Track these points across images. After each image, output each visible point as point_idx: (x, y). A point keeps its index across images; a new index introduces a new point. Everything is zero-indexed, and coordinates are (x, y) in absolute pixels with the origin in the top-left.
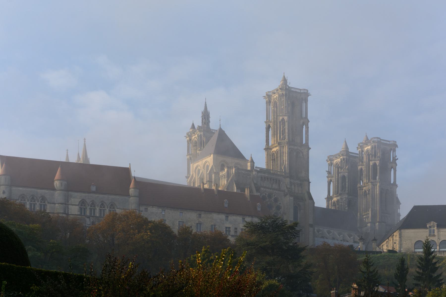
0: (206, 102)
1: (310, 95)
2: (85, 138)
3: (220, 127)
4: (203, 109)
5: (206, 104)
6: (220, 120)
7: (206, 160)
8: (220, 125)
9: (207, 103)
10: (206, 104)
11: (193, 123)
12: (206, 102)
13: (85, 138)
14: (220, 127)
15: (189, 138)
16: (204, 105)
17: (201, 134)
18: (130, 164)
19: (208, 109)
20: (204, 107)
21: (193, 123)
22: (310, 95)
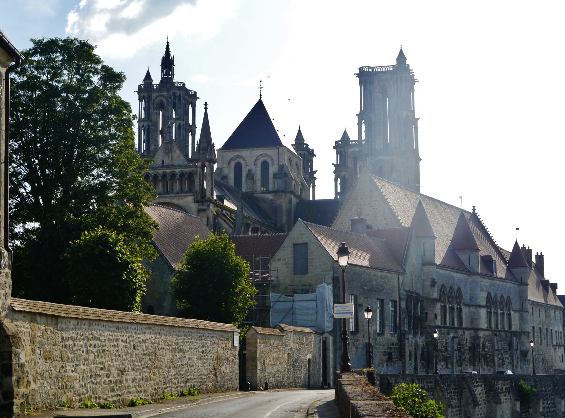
0: (168, 43)
1: (417, 81)
2: (206, 103)
3: (261, 98)
4: (163, 52)
5: (168, 46)
6: (261, 88)
7: (267, 153)
8: (261, 95)
9: (169, 44)
10: (168, 46)
11: (148, 70)
12: (168, 43)
13: (206, 103)
14: (261, 98)
15: (147, 95)
16: (166, 47)
17: (180, 95)
18: (474, 207)
19: (171, 53)
21: (148, 70)
22: (417, 81)
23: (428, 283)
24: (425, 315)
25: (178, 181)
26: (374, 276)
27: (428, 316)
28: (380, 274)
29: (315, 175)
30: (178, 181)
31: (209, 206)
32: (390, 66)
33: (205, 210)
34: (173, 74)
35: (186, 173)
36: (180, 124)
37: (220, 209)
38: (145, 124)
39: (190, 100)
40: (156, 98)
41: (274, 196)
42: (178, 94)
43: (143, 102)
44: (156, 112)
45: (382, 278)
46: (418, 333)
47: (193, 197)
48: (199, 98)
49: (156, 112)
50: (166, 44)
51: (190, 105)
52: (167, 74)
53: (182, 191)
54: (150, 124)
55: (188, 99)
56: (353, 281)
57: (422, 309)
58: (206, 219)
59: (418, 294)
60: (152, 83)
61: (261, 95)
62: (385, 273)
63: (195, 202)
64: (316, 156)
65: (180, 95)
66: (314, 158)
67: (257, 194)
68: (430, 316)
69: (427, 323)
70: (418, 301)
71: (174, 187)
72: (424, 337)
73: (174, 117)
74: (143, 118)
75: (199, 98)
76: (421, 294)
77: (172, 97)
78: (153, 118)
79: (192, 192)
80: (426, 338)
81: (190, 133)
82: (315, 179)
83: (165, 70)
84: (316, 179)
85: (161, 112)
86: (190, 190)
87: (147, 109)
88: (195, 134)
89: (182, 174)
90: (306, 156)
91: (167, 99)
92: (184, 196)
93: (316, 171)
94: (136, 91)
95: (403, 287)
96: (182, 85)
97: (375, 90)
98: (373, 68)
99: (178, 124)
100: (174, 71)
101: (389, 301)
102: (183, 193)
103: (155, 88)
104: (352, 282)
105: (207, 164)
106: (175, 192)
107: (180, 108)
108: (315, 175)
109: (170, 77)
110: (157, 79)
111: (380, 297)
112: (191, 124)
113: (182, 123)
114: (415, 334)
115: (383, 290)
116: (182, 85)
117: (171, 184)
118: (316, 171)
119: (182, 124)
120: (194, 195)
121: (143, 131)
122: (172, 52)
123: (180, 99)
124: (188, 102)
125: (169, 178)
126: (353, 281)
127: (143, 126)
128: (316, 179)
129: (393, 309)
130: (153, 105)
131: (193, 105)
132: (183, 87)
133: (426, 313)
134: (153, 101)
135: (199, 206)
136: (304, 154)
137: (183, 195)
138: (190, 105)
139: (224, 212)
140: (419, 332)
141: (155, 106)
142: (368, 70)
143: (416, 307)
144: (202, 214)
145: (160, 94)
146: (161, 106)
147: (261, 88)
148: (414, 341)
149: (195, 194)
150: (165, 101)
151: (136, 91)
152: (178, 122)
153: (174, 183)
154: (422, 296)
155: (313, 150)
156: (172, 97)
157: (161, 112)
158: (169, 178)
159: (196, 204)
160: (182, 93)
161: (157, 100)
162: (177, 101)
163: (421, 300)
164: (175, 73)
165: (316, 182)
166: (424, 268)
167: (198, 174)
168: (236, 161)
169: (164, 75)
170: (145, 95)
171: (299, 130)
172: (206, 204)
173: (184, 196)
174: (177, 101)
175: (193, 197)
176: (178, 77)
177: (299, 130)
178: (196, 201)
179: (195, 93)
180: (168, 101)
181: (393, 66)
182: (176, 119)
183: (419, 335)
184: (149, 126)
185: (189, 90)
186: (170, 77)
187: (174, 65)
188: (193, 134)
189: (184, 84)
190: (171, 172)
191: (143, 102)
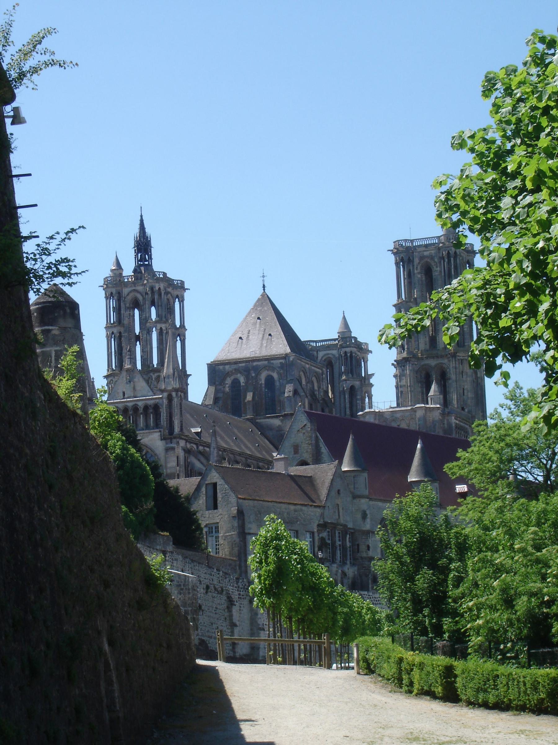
0: (141, 216)
4: (135, 230)
6: (263, 276)
8: (264, 287)
12: (141, 216)
16: (139, 222)
17: (159, 289)
19: (147, 230)
20: (138, 226)
23: (359, 516)
24: (356, 547)
25: (141, 416)
26: (286, 509)
27: (360, 547)
28: (292, 507)
29: (372, 381)
30: (141, 416)
31: (178, 443)
32: (434, 237)
33: (173, 449)
34: (150, 258)
35: (150, 406)
36: (161, 328)
37: (195, 446)
38: (115, 330)
39: (175, 293)
40: (128, 295)
41: (282, 421)
42: (157, 288)
43: (111, 300)
44: (130, 314)
45: (295, 511)
46: (346, 564)
47: (159, 434)
48: (187, 289)
49: (130, 314)
50: (140, 218)
51: (177, 300)
52: (143, 259)
53: (147, 427)
54: (122, 330)
55: (172, 292)
56: (260, 514)
57: (353, 540)
58: (175, 459)
59: (345, 526)
60: (121, 274)
61: (264, 287)
62: (298, 507)
63: (161, 440)
64: (371, 352)
65: (159, 289)
66: (370, 356)
67: (260, 419)
68: (363, 548)
69: (359, 555)
70: (346, 533)
71: (138, 422)
72: (356, 568)
73: (154, 320)
74: (112, 322)
75: (187, 289)
76: (350, 525)
77: (149, 293)
78: (126, 321)
79: (159, 428)
80: (358, 569)
81: (178, 338)
82: (372, 385)
83: (139, 255)
84: (373, 385)
85: (137, 312)
86: (157, 425)
87: (118, 310)
88: (184, 339)
89: (146, 408)
90: (354, 354)
91: (143, 296)
92: (149, 432)
93: (373, 374)
94: (101, 286)
95: (323, 519)
96: (161, 276)
97: (416, 271)
98: (412, 241)
99: (158, 328)
100: (151, 255)
101: (304, 532)
102: (149, 429)
103: (126, 280)
104: (259, 515)
105: (174, 394)
106: (139, 428)
107: (161, 306)
108: (372, 381)
109: (147, 263)
110: (128, 270)
111: (292, 528)
112: (178, 324)
113: (163, 326)
114: (344, 563)
115: (297, 521)
116: (161, 276)
117: (134, 419)
118: (373, 374)
119: (164, 328)
120: (160, 431)
121: (113, 339)
122: (148, 230)
123: (160, 295)
124: (172, 297)
125: (131, 413)
126: (260, 514)
127: (113, 333)
128: (373, 385)
129: (311, 540)
130: (125, 304)
131: (181, 300)
132: (165, 279)
133: (358, 545)
134: (125, 298)
135: (167, 443)
136: (351, 352)
137: (147, 431)
138: (177, 300)
139: (201, 448)
140: (348, 562)
141: (128, 305)
142: (405, 244)
143: (344, 539)
144: (171, 453)
145: (134, 288)
146: (136, 304)
147: (263, 276)
148: (340, 571)
149: (162, 430)
150: (140, 298)
151: (101, 286)
152: (159, 326)
153: (138, 418)
154: (350, 528)
155: (366, 344)
156: (149, 293)
157: (137, 312)
158: (131, 413)
159: (164, 442)
160: (162, 286)
161: (129, 298)
162: (156, 297)
163: (352, 533)
164: (153, 257)
165: (374, 391)
166: (355, 501)
167: (164, 406)
168: (232, 378)
169: (138, 261)
170: (114, 291)
171: (344, 318)
172: (174, 441)
173: (149, 432)
174: (156, 297)
175: (159, 434)
176: (158, 265)
177: (344, 318)
178: (163, 438)
179: (182, 283)
180: (144, 299)
181: (438, 237)
182: (156, 322)
183: (348, 566)
184: (120, 333)
185: (174, 280)
186: (147, 263)
187: (151, 247)
188: (182, 339)
189: (165, 274)
190: (134, 405)
191: (111, 300)
